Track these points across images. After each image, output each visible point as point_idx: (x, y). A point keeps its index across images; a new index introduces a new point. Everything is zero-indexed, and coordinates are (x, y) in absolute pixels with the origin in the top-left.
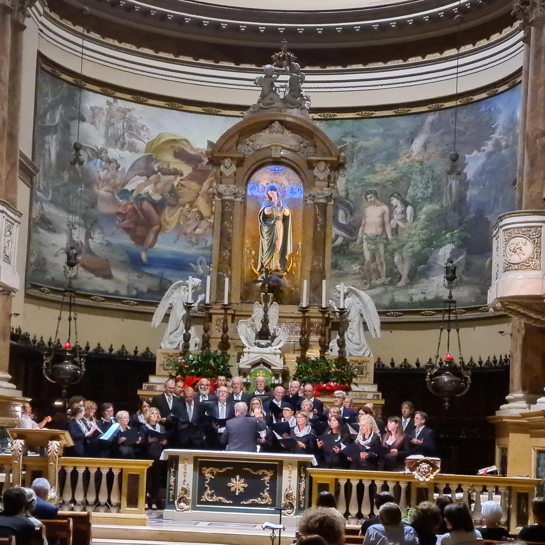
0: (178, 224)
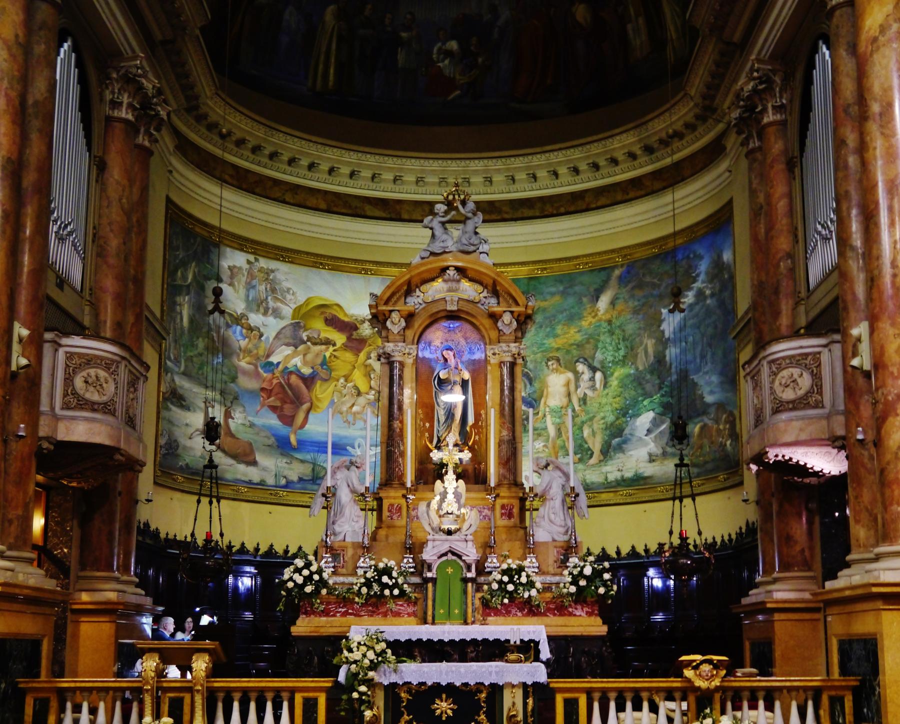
0: (332, 402)
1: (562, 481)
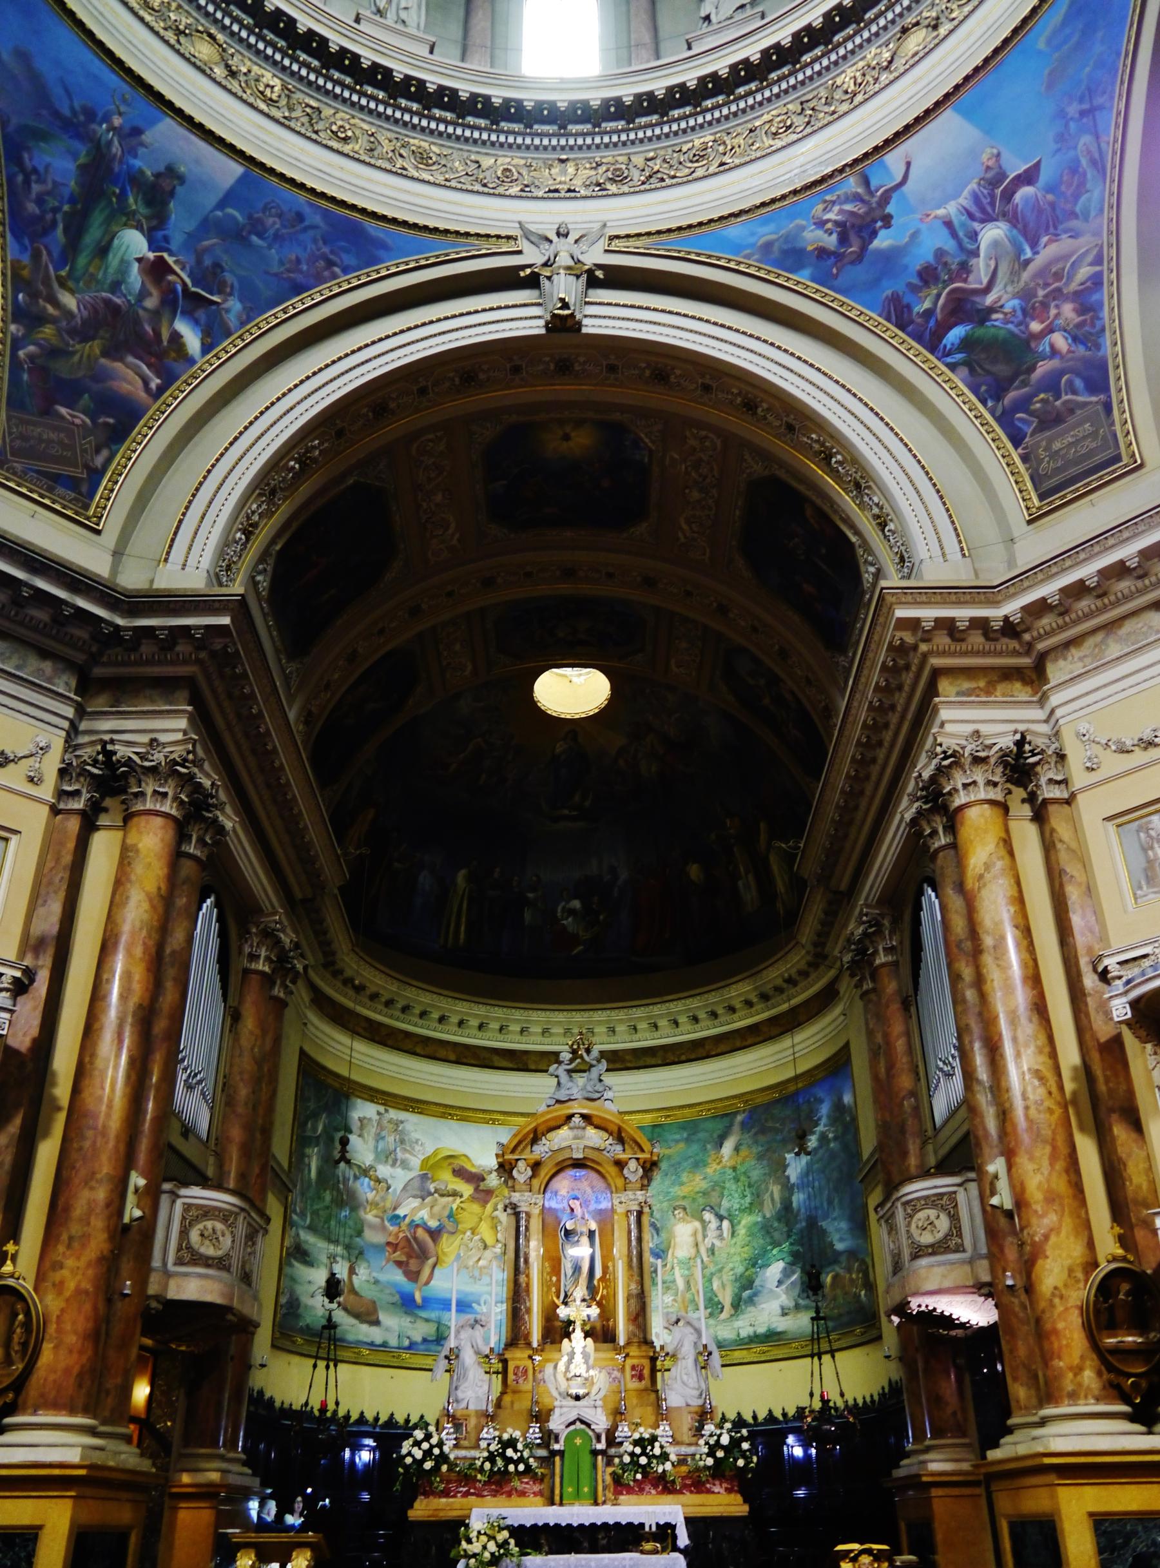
0: (458, 1257)
1: (693, 1338)
